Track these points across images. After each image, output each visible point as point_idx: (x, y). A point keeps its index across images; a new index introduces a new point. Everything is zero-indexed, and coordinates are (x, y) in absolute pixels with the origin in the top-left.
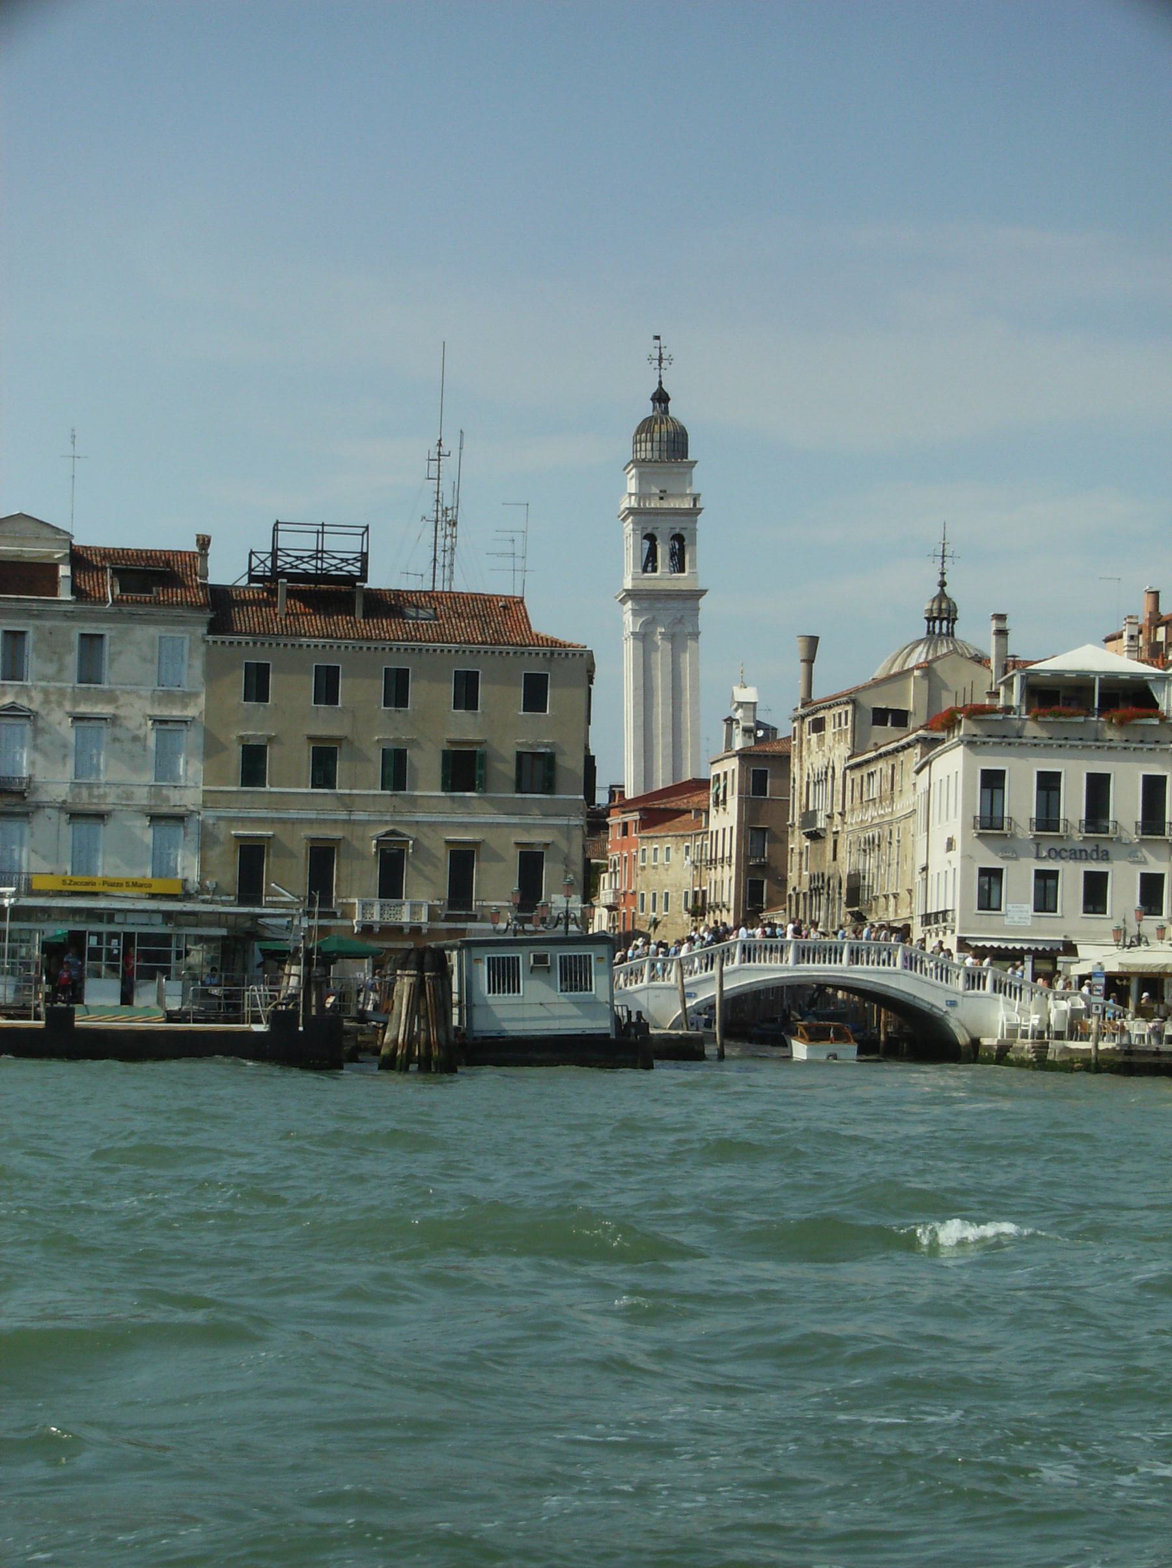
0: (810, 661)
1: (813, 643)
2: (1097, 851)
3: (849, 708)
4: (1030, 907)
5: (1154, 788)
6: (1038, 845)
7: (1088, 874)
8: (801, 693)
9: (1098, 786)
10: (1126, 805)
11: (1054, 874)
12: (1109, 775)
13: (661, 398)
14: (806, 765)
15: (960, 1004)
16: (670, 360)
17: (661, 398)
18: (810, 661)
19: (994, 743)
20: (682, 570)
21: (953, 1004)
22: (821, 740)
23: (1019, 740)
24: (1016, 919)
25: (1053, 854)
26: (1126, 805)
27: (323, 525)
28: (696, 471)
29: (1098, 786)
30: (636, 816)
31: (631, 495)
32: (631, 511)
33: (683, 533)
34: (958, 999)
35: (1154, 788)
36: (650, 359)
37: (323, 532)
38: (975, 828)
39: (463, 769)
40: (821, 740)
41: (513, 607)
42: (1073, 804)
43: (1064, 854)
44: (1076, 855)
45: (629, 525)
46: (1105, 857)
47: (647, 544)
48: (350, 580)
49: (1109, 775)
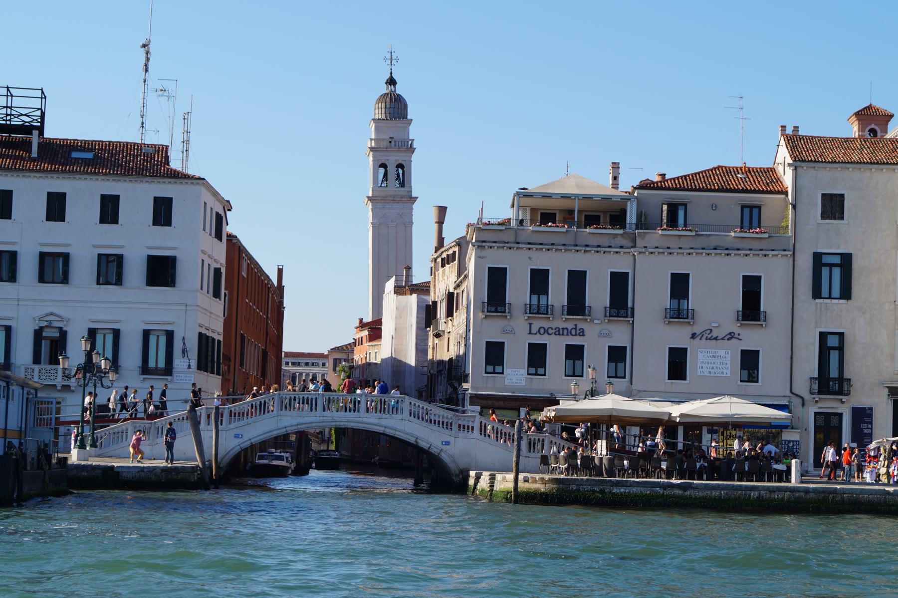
0: (440, 223)
1: (442, 211)
2: (576, 329)
3: (456, 249)
4: (524, 371)
5: (620, 284)
6: (530, 324)
7: (568, 347)
8: (434, 243)
9: (577, 280)
10: (598, 294)
11: (544, 346)
12: (585, 272)
13: (392, 82)
14: (437, 290)
15: (452, 443)
16: (397, 60)
17: (392, 82)
18: (440, 223)
19: (498, 247)
20: (402, 185)
21: (447, 443)
22: (444, 272)
23: (517, 245)
24: (514, 380)
25: (542, 331)
26: (598, 294)
27: (8, 88)
28: (412, 128)
29: (577, 280)
30: (365, 333)
31: (371, 140)
32: (372, 149)
33: (404, 163)
34: (452, 440)
35: (620, 284)
36: (385, 59)
37: (12, 96)
38: (483, 312)
39: (110, 269)
40: (444, 272)
41: (162, 152)
42: (558, 292)
43: (550, 331)
44: (559, 332)
45: (371, 158)
46: (582, 333)
47: (382, 171)
48: (26, 129)
49: (585, 272)
